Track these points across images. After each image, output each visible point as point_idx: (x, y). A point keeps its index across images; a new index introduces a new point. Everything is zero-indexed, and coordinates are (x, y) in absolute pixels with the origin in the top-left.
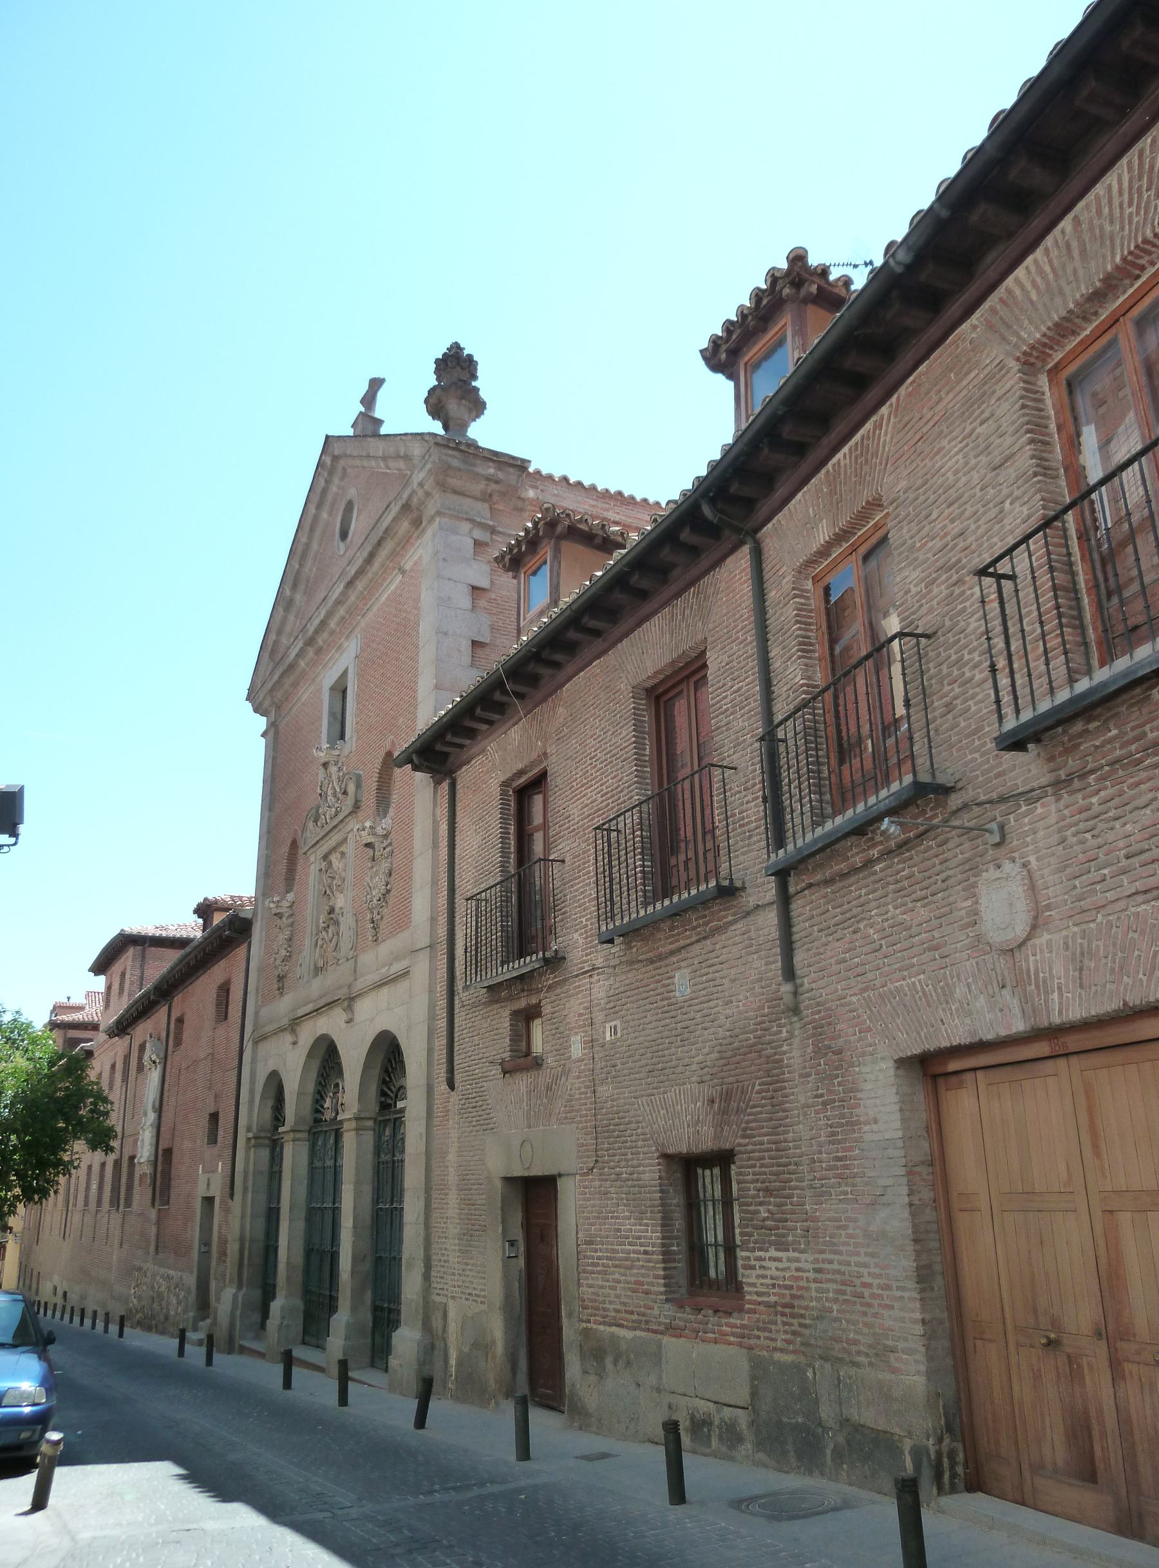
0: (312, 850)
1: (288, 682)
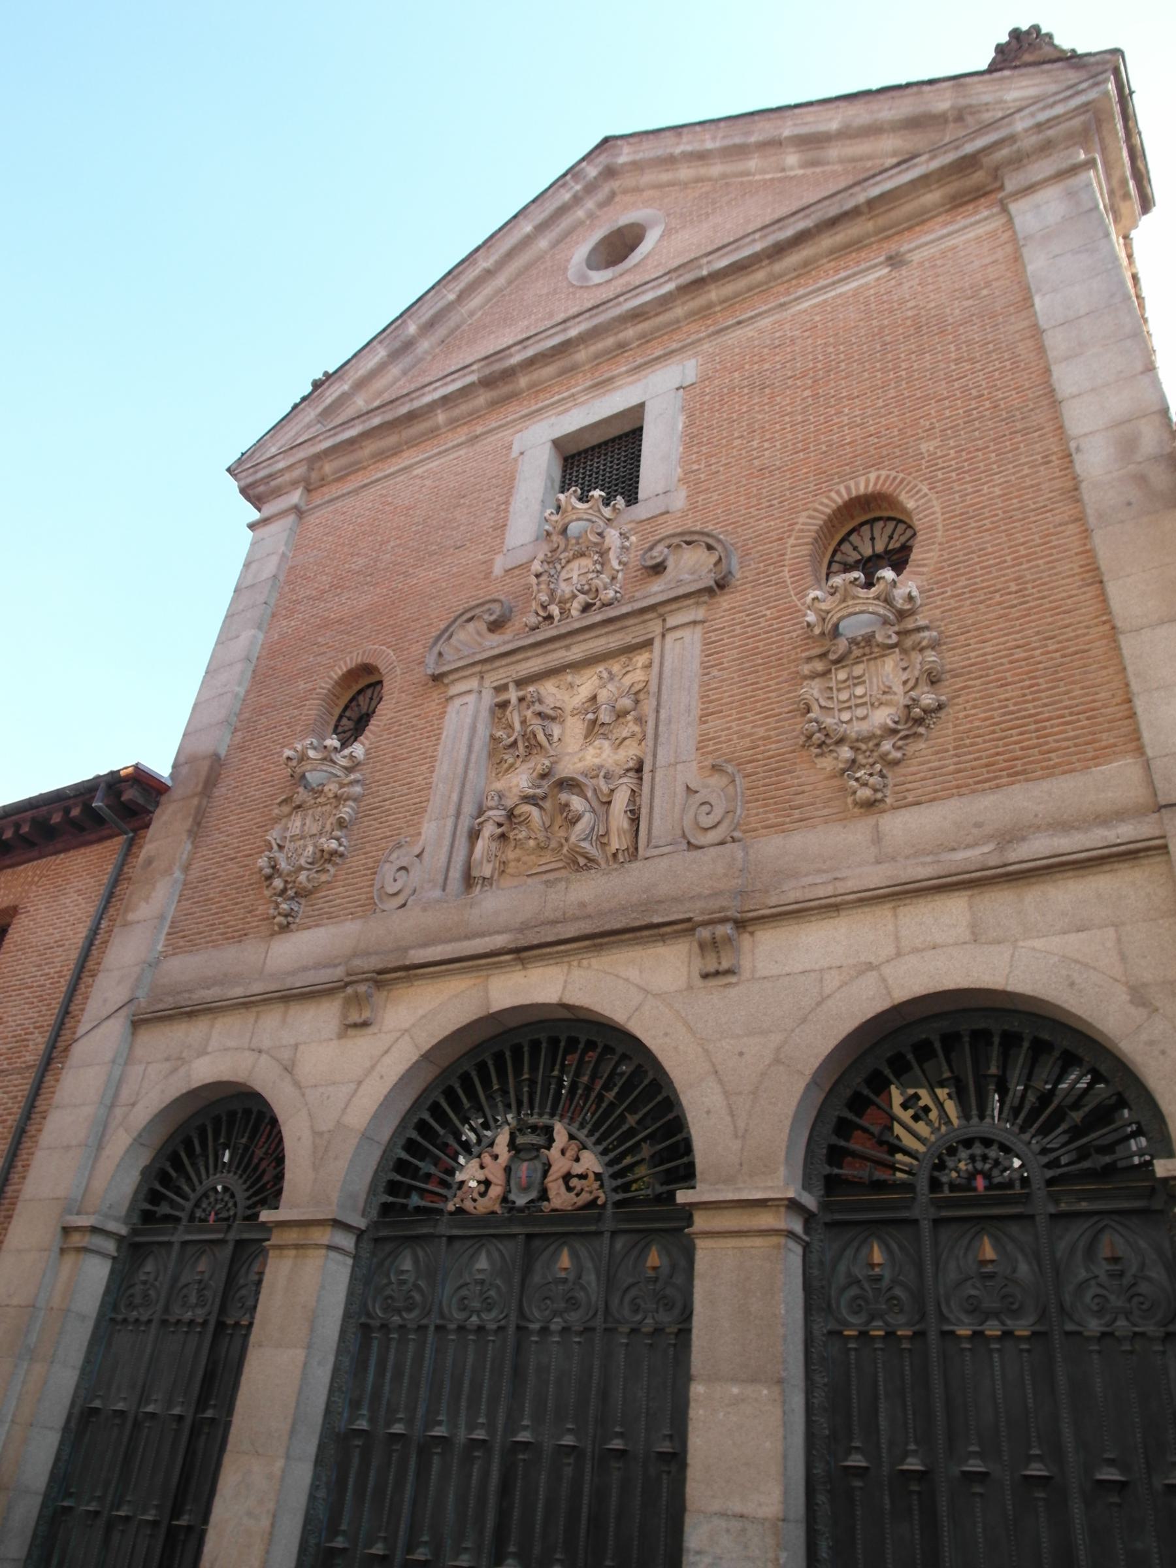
0: (477, 669)
1: (370, 447)
